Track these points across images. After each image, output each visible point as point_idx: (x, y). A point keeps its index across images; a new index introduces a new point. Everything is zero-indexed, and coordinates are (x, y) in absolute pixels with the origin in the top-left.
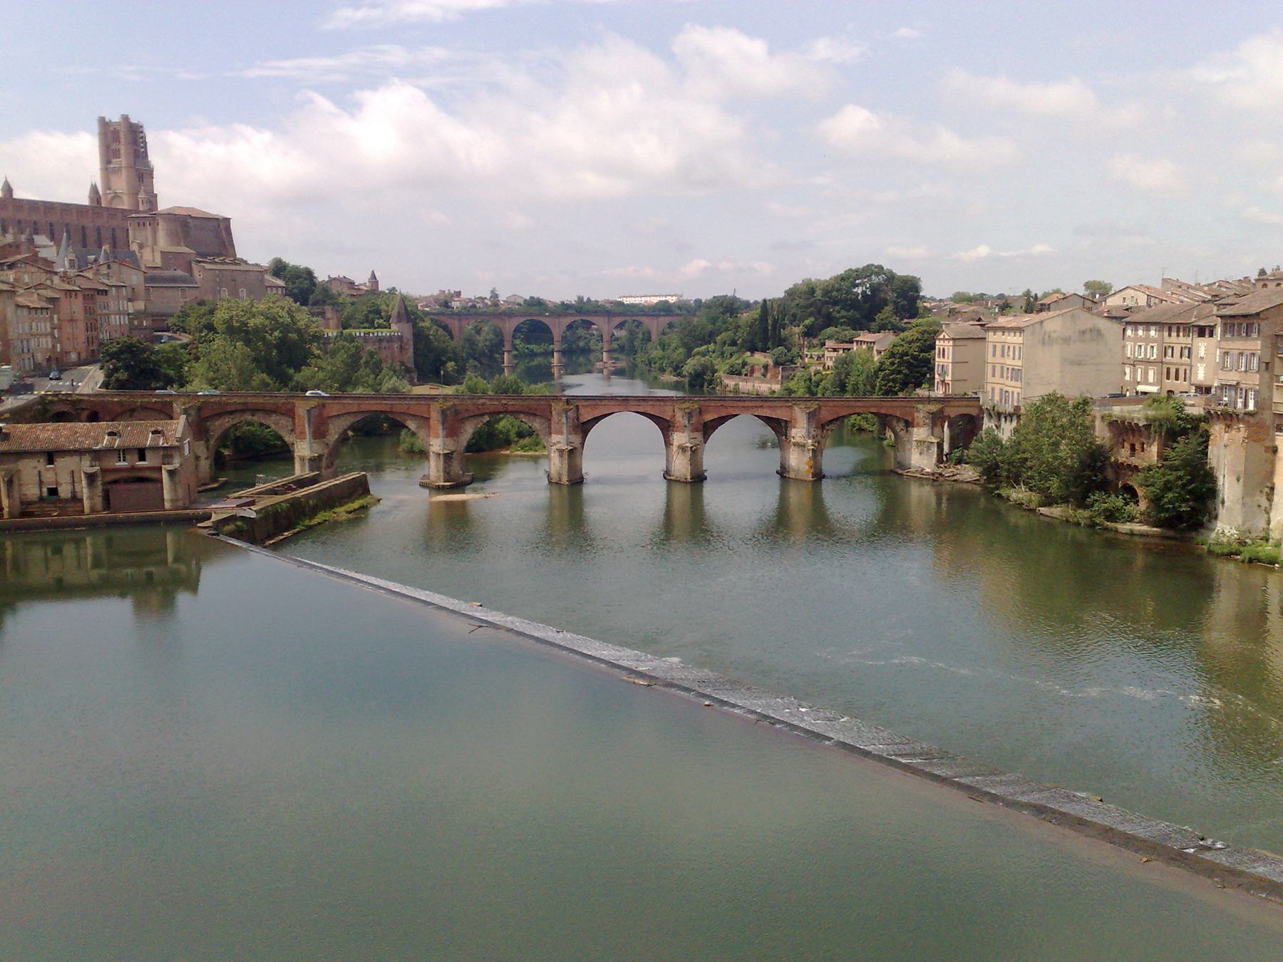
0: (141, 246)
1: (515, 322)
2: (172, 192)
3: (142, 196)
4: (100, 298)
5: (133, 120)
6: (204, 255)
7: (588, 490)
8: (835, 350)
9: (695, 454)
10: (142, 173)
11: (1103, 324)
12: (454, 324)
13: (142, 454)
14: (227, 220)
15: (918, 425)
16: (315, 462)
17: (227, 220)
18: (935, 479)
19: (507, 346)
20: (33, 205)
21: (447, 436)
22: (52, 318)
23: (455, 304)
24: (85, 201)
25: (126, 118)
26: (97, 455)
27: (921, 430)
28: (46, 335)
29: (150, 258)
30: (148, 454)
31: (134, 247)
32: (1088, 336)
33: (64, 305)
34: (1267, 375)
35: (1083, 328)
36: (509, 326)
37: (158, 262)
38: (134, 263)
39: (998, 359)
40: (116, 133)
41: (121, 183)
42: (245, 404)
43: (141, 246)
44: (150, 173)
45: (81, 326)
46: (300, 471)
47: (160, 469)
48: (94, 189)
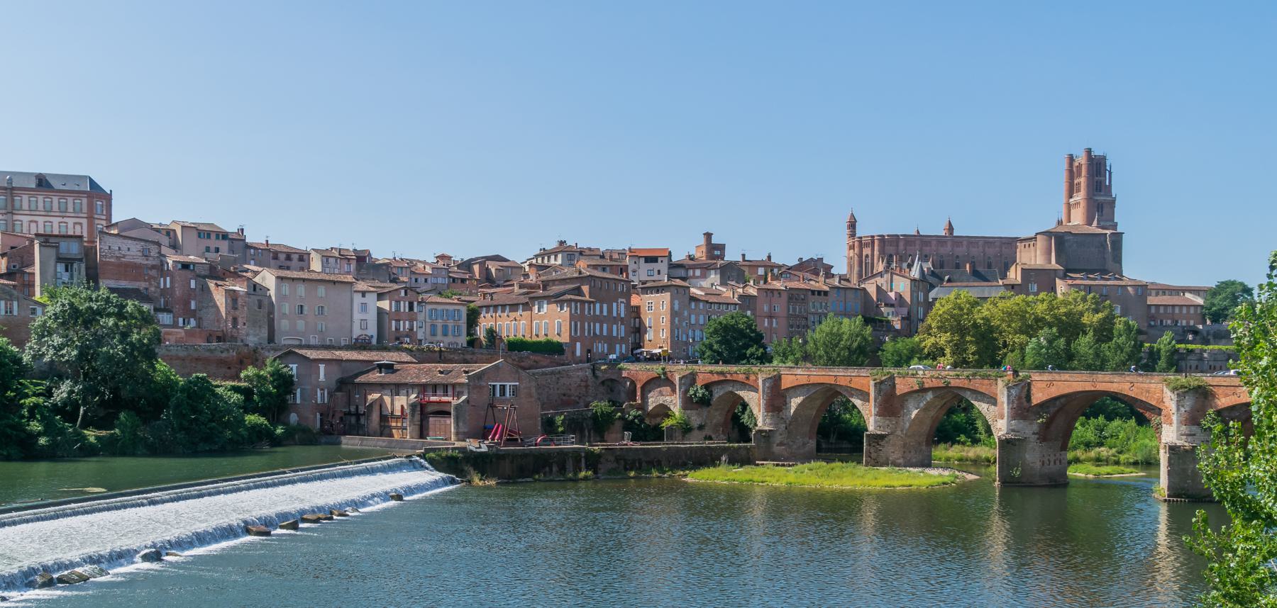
5: (1097, 152)
20: (972, 241)
21: (879, 414)
25: (1089, 151)
26: (423, 388)
37: (1019, 279)
42: (722, 373)
44: (1113, 202)
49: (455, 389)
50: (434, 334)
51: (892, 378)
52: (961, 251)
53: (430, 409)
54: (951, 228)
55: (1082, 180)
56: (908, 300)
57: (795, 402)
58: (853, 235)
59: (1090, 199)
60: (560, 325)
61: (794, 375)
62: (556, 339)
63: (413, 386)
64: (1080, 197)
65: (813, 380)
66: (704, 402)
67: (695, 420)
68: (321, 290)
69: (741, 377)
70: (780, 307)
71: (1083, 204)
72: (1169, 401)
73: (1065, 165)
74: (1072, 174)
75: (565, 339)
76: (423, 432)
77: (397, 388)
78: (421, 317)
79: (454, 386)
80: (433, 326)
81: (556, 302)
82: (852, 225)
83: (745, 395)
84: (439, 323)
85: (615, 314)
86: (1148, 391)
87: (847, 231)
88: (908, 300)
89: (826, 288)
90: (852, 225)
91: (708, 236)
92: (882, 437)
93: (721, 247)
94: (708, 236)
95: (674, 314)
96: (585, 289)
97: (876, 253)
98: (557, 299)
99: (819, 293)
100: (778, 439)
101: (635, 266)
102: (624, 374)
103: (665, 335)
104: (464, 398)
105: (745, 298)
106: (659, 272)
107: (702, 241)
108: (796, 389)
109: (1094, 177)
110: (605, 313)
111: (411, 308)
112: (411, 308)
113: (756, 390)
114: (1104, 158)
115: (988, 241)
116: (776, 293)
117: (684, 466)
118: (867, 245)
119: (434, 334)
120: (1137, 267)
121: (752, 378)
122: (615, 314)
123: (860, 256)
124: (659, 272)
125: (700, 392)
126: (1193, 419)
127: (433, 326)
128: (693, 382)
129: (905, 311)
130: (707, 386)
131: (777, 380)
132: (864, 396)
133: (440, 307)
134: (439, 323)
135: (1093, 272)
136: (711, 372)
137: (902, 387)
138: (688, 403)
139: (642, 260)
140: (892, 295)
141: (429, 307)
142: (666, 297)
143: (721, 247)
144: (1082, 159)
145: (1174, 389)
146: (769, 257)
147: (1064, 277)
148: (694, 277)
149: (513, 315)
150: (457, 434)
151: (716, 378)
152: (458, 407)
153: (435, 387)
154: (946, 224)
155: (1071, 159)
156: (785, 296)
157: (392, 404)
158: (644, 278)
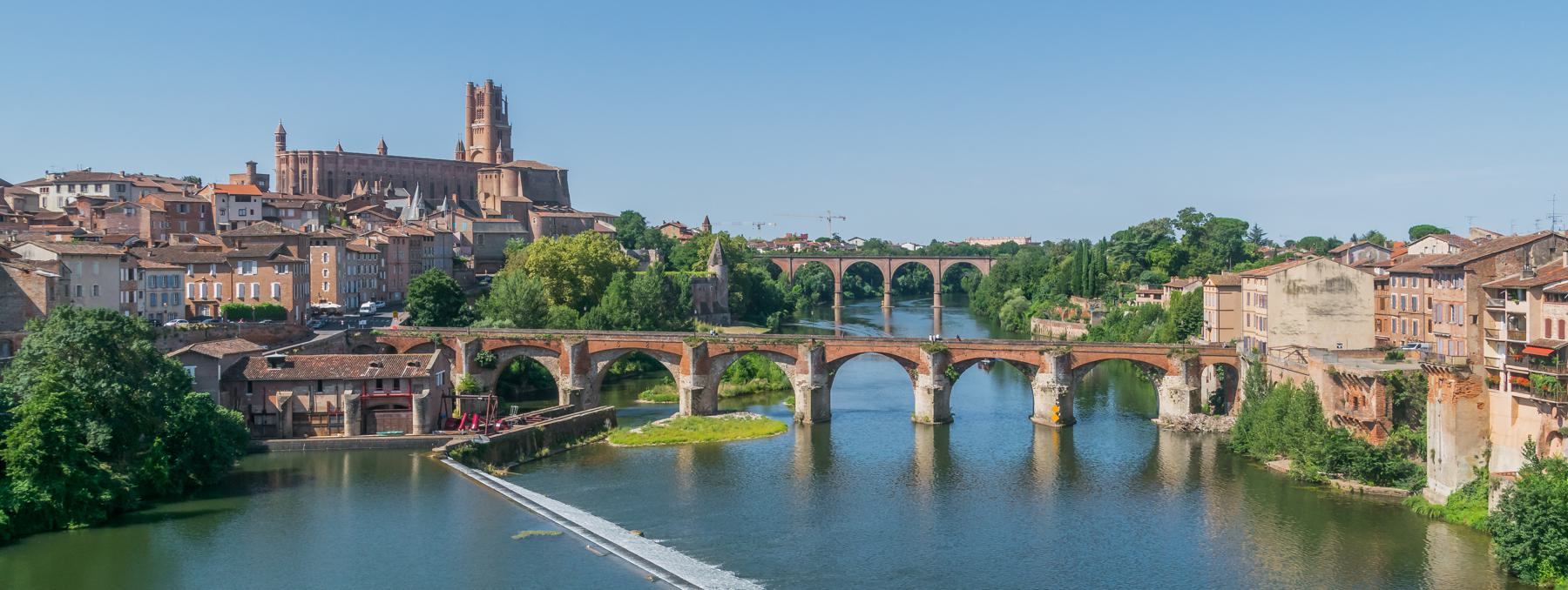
0: (487, 196)
1: (846, 264)
2: (528, 149)
3: (499, 150)
4: (425, 244)
5: (496, 84)
6: (541, 204)
7: (835, 426)
8: (1147, 295)
9: (940, 398)
10: (500, 133)
11: (1351, 273)
12: (786, 266)
13: (396, 383)
14: (564, 173)
15: (1172, 374)
16: (575, 396)
17: (564, 173)
18: (1186, 432)
19: (838, 287)
20: (404, 161)
21: (696, 373)
23: (797, 246)
24: (453, 158)
25: (491, 83)
26: (361, 384)
27: (1175, 379)
29: (491, 206)
30: (402, 384)
31: (481, 198)
32: (1336, 285)
33: (392, 253)
34: (1475, 330)
35: (1330, 276)
36: (839, 268)
37: (499, 210)
38: (472, 211)
39: (1252, 307)
40: (481, 95)
41: (482, 142)
42: (517, 339)
43: (487, 196)
45: (406, 268)
46: (563, 401)
47: (410, 399)
48: (461, 145)
49: (414, 384)
50: (153, 305)
51: (705, 344)
52: (393, 170)
53: (371, 404)
54: (385, 148)
55: (486, 108)
56: (470, 239)
57: (601, 365)
58: (283, 148)
59: (492, 126)
60: (279, 289)
61: (602, 342)
62: (276, 304)
63: (345, 382)
64: (483, 123)
65: (622, 345)
66: (491, 366)
67: (480, 384)
68: (96, 265)
69: (539, 343)
70: (404, 253)
71: (486, 131)
72: (926, 358)
73: (467, 93)
74: (474, 99)
75: (287, 303)
76: (366, 426)
77: (320, 385)
78: (141, 286)
79: (410, 380)
80: (153, 295)
81: (272, 265)
82: (282, 138)
83: (548, 362)
84: (159, 291)
88: (471, 240)
90: (282, 138)
91: (252, 165)
92: (700, 391)
93: (266, 178)
94: (252, 165)
95: (339, 267)
96: (293, 249)
97: (315, 169)
98: (270, 260)
100: (586, 397)
101: (223, 205)
102: (379, 340)
103: (328, 289)
104: (426, 392)
105: (380, 246)
107: (246, 170)
108: (601, 354)
109: (492, 106)
111: (131, 277)
112: (131, 277)
113: (557, 354)
115: (417, 162)
117: (587, 434)
118: (304, 161)
119: (153, 305)
120: (582, 201)
121: (553, 343)
123: (296, 171)
125: (489, 358)
126: (940, 371)
127: (153, 295)
128: (479, 349)
129: (469, 250)
130: (493, 351)
131: (586, 344)
132: (676, 358)
133: (159, 274)
134: (159, 291)
135: (551, 204)
136: (503, 339)
137: (713, 351)
138: (476, 367)
140: (457, 235)
141: (149, 274)
142: (332, 249)
143: (266, 178)
144: (482, 87)
145: (930, 352)
147: (533, 209)
148: (287, 217)
149: (203, 276)
150: (422, 427)
151: (508, 344)
152: (422, 402)
153: (379, 383)
154: (378, 143)
155: (472, 88)
157: (312, 401)
158: (235, 217)
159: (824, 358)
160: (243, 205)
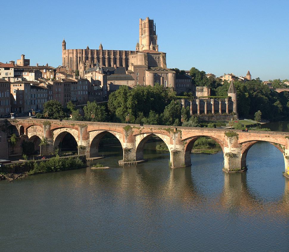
22: (48, 93)
28: (44, 98)
85: (6, 97)
86: (220, 136)
87: (63, 48)
89: (76, 81)
91: (24, 56)
99: (74, 83)
106: (10, 74)
110: (3, 97)
114: (153, 21)
116: (60, 84)
122: (6, 97)
124: (10, 74)
139: (3, 69)
146: (47, 65)
154: (99, 45)
156: (63, 85)
159: (181, 138)
160: (7, 71)
